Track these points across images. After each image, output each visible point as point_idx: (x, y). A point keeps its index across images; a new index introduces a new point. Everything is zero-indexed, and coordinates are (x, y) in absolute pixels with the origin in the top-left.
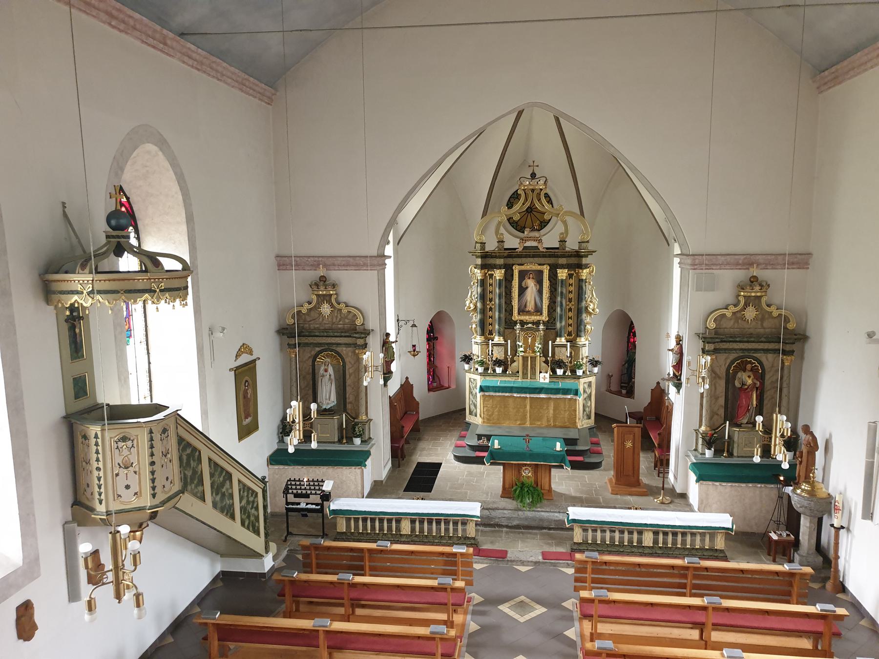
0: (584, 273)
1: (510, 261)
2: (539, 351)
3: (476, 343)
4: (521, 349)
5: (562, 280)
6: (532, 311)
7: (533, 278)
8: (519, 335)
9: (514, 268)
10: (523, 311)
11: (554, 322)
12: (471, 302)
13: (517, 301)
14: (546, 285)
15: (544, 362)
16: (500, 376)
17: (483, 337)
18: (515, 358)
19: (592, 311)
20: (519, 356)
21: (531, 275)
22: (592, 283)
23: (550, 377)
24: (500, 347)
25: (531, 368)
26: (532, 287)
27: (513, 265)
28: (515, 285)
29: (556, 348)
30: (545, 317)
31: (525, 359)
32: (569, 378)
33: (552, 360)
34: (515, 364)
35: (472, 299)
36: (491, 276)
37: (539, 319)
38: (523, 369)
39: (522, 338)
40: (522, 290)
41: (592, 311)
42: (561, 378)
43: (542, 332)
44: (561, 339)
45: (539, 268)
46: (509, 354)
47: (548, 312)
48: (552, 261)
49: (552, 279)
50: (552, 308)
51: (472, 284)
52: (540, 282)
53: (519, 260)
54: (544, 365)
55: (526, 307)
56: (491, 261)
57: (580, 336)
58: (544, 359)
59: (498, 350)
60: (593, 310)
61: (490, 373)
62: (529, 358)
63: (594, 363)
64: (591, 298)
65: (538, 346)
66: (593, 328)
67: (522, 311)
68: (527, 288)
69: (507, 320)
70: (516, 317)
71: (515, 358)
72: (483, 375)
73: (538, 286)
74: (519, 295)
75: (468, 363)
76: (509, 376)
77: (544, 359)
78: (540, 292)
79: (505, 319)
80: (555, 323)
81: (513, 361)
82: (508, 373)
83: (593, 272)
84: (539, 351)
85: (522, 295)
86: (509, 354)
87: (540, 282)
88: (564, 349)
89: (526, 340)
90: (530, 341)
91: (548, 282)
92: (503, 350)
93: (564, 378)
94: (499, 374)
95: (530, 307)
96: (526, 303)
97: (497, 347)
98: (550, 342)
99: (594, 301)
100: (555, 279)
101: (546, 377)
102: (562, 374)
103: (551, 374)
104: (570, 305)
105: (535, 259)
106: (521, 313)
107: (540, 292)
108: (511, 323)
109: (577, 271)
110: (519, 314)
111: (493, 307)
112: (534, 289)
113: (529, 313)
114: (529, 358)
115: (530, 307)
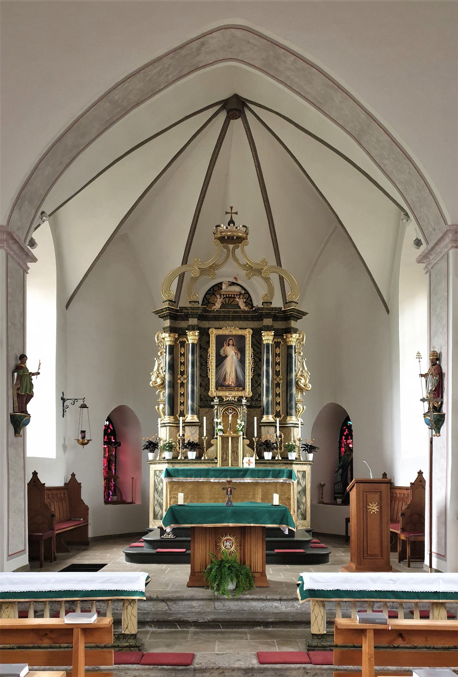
0: (293, 339)
1: (205, 324)
2: (242, 430)
3: (164, 425)
4: (220, 427)
5: (268, 345)
6: (233, 385)
7: (233, 345)
8: (217, 412)
9: (210, 331)
10: (222, 386)
11: (259, 399)
12: (158, 376)
13: (214, 374)
14: (249, 353)
15: (247, 445)
16: (192, 463)
17: (172, 417)
18: (212, 442)
19: (303, 386)
20: (217, 438)
21: (231, 341)
22: (302, 354)
23: (256, 463)
24: (193, 427)
25: (233, 452)
26: (233, 356)
27: (209, 328)
28: (212, 353)
29: (263, 428)
30: (248, 392)
31: (224, 440)
32: (279, 463)
33: (258, 440)
34: (212, 448)
35: (160, 373)
36: (183, 344)
37: (240, 395)
38: (223, 454)
39: (220, 414)
40: (221, 360)
41: (303, 386)
42: (270, 463)
43: (245, 407)
44: (268, 417)
45: (240, 332)
46: (205, 435)
47: (252, 387)
48: (256, 324)
49: (255, 348)
50: (256, 382)
51: (159, 354)
52: (241, 350)
53: (217, 324)
54: (247, 448)
55: (225, 381)
56: (183, 324)
57: (291, 415)
58: (247, 442)
59: (191, 432)
60: (304, 385)
61: (181, 459)
62: (230, 439)
63: (309, 448)
64: (302, 371)
65: (241, 423)
66: (305, 407)
67: (220, 385)
68: (226, 357)
69: (202, 397)
70: (213, 391)
71: (212, 442)
72: (172, 463)
73: (239, 355)
74: (217, 366)
75: (152, 451)
76: (204, 463)
77: (247, 442)
78: (242, 362)
79: (200, 395)
80: (260, 401)
81: (210, 445)
82: (203, 458)
83: (303, 341)
84: (242, 430)
85: (220, 366)
86: (205, 435)
87: (241, 350)
88: (272, 429)
89: (225, 417)
90: (230, 418)
91: (251, 350)
92: (198, 432)
93: (273, 463)
94: (192, 460)
95: (231, 380)
96: (225, 375)
97: (190, 427)
98: (255, 418)
99: (305, 374)
100: (260, 347)
101: (251, 461)
102: (270, 458)
103: (258, 458)
104: (278, 379)
105: (235, 322)
106: (219, 388)
107: (242, 362)
108: (207, 400)
109: (285, 337)
110: (217, 389)
111: (185, 381)
112: (235, 358)
113: (229, 388)
114: (230, 439)
115: (231, 380)
